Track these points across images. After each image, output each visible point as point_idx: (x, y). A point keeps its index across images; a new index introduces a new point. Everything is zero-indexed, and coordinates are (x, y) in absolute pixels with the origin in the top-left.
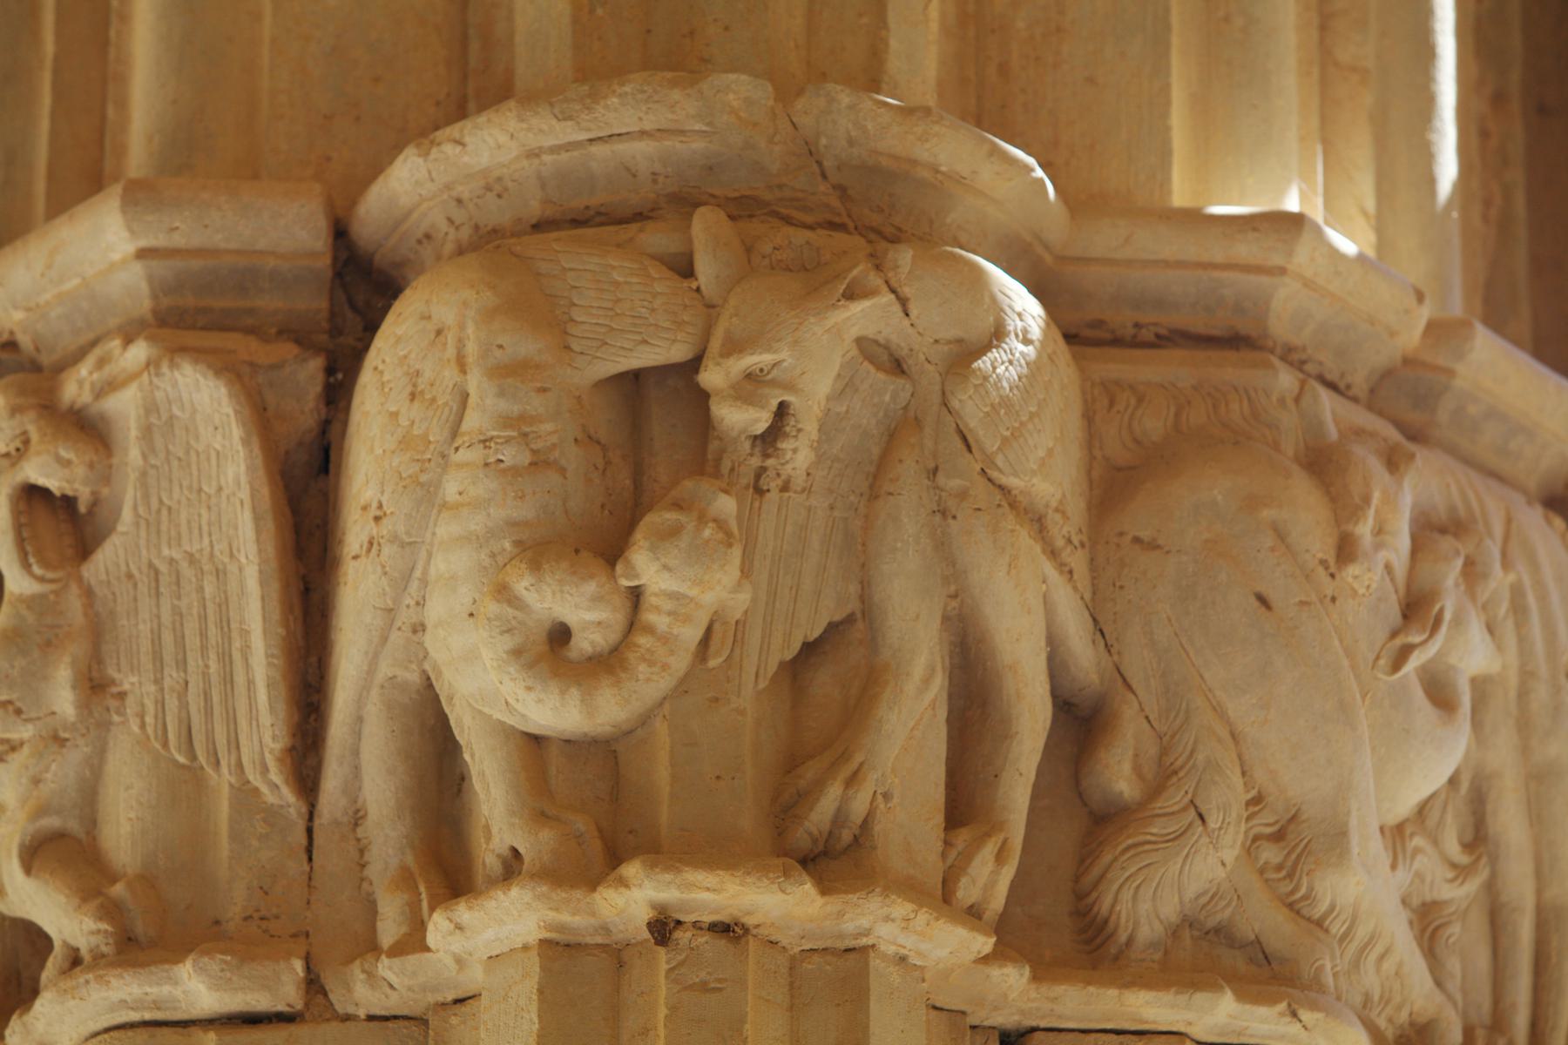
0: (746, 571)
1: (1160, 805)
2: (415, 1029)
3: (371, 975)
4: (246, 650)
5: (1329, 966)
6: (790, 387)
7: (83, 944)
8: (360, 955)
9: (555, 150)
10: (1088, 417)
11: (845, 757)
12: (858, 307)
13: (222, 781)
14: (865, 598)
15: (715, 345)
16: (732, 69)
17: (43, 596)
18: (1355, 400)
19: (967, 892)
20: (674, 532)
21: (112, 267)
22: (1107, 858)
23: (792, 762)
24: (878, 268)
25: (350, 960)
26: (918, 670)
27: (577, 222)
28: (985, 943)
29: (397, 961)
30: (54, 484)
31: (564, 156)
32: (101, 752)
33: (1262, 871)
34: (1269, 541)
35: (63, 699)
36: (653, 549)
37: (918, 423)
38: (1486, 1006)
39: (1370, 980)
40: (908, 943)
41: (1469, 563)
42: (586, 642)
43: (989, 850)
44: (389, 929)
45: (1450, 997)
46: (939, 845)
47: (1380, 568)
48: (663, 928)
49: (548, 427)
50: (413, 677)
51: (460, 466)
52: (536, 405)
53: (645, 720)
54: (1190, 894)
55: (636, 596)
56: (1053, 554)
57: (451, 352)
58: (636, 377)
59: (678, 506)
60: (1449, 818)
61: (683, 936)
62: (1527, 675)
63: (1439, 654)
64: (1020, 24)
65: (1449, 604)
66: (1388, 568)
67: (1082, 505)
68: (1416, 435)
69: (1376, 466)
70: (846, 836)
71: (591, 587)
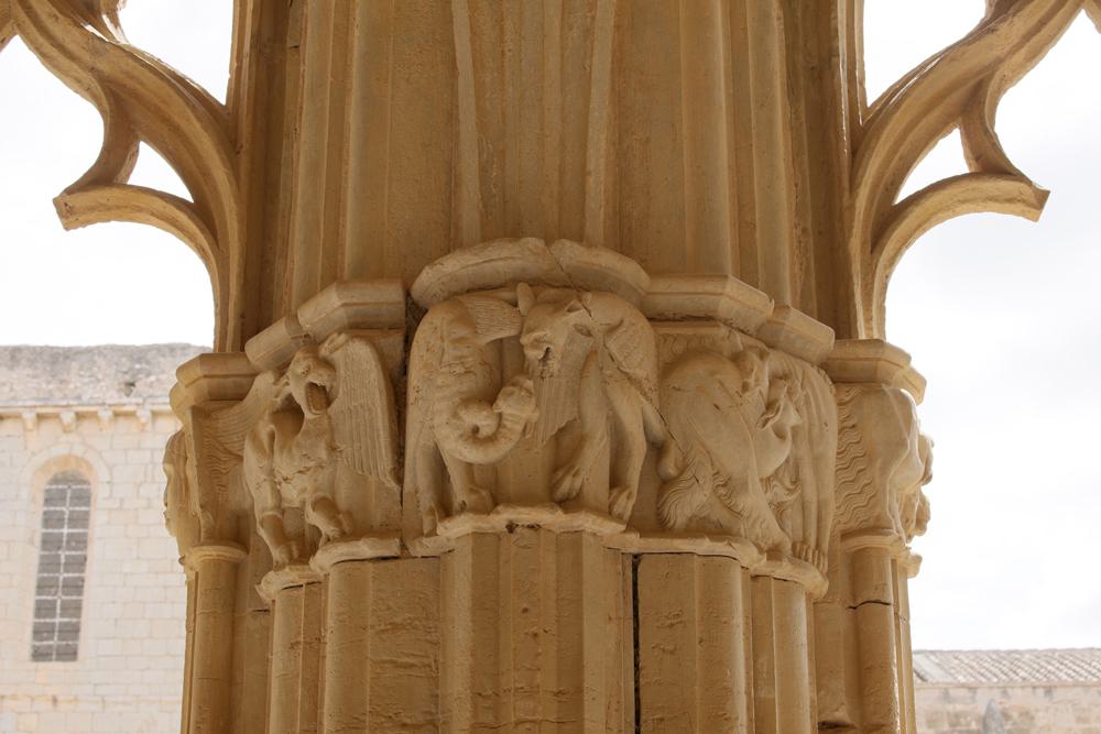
0: (537, 406)
1: (682, 478)
2: (435, 560)
3: (421, 543)
4: (378, 436)
5: (742, 527)
6: (550, 343)
7: (331, 534)
8: (418, 537)
9: (473, 265)
10: (657, 346)
11: (573, 467)
12: (573, 314)
13: (372, 479)
14: (579, 412)
15: (524, 330)
16: (532, 235)
17: (315, 419)
18: (751, 335)
19: (617, 510)
20: (512, 393)
21: (336, 309)
22: (666, 496)
23: (555, 468)
24: (580, 301)
25: (414, 539)
26: (598, 435)
27: (481, 289)
28: (623, 527)
29: (428, 539)
30: (317, 382)
31: (361, 307)
32: (335, 470)
33: (719, 497)
34: (718, 385)
35: (323, 454)
36: (505, 400)
37: (596, 352)
38: (801, 533)
39: (758, 530)
40: (596, 528)
41: (789, 388)
42: (485, 432)
43: (626, 494)
44: (426, 529)
45: (787, 534)
46: (607, 495)
47: (757, 393)
48: (511, 527)
49: (470, 359)
50: (431, 444)
51: (442, 373)
52: (466, 352)
53: (505, 457)
54: (695, 505)
55: (500, 415)
56: (645, 394)
57: (439, 335)
58: (501, 340)
59: (514, 385)
60: (786, 474)
61: (518, 530)
62: (810, 425)
63: (780, 420)
64: (635, 214)
65: (782, 403)
66: (760, 392)
67: (655, 376)
68: (772, 346)
69: (755, 357)
70: (574, 494)
71: (485, 413)
